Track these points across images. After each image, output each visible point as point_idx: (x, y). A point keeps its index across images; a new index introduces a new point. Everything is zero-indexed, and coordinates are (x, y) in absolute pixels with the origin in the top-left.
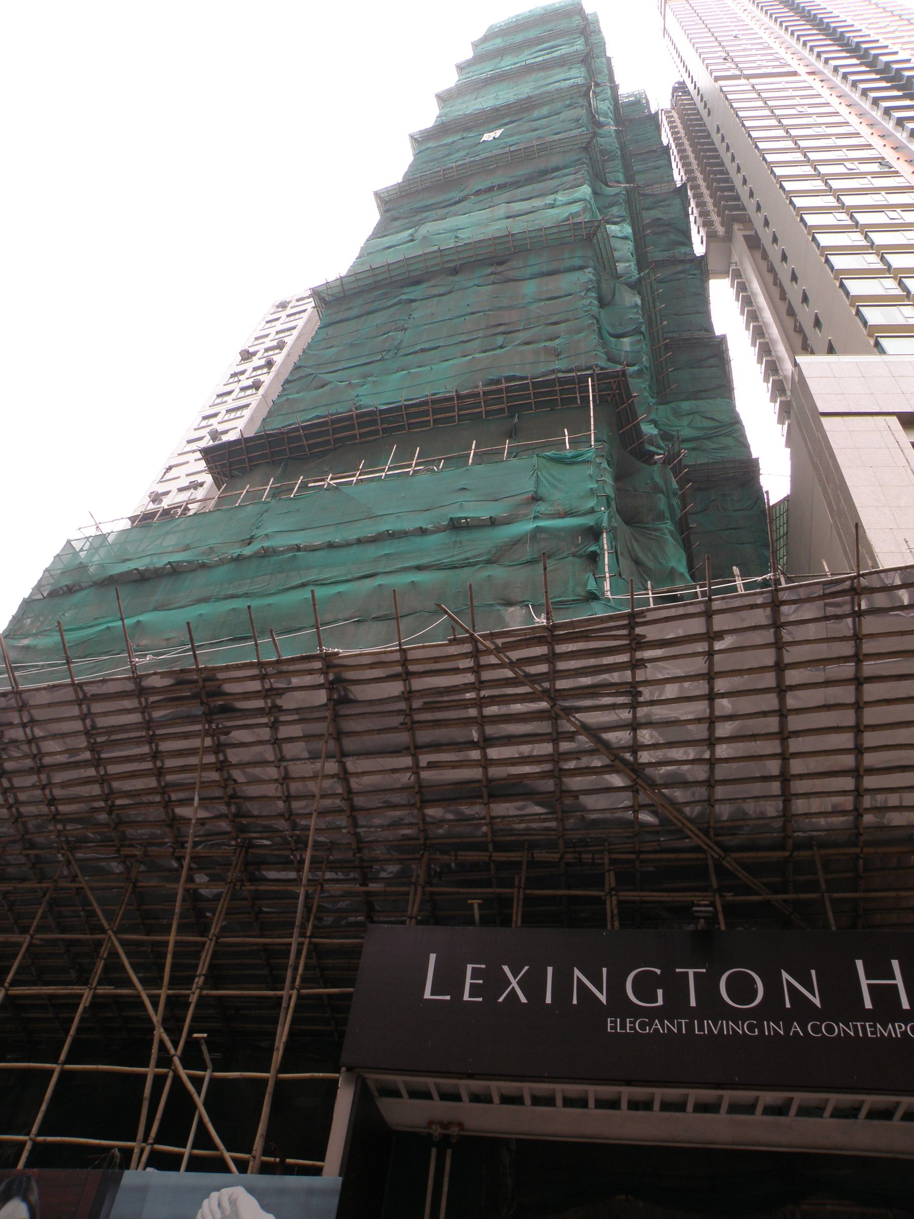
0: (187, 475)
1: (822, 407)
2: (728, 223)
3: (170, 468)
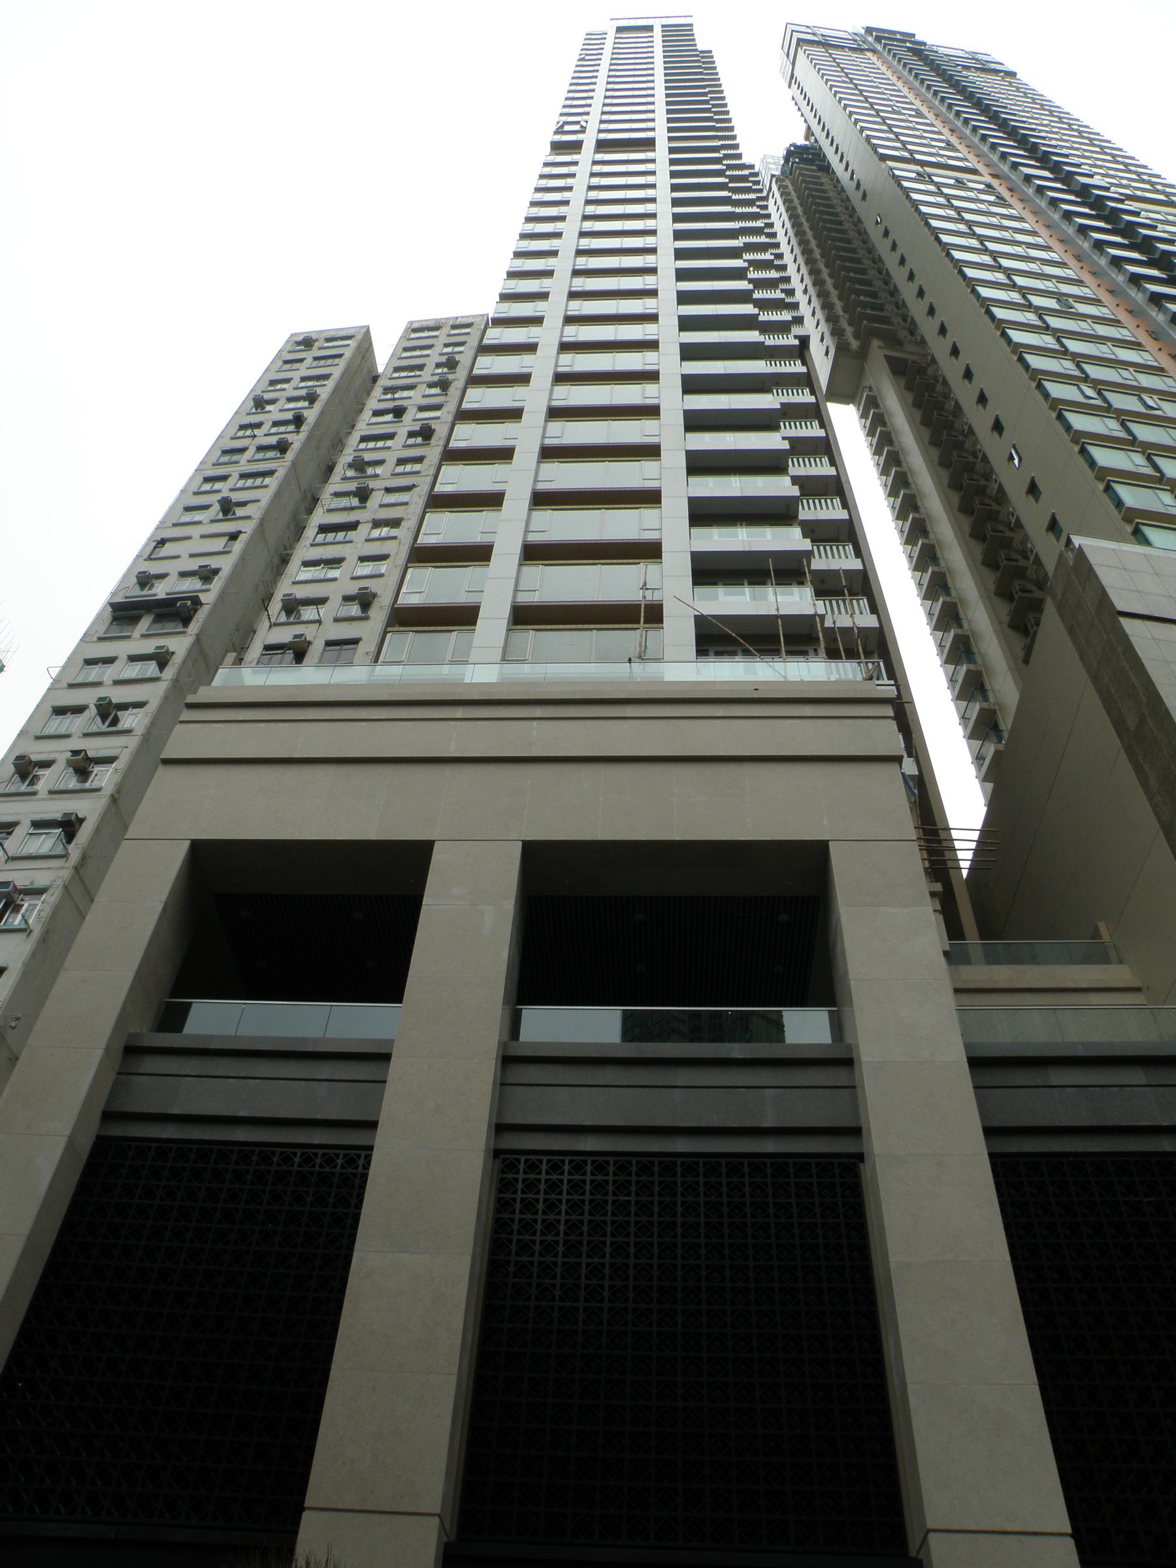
0: (191, 556)
1: (1120, 605)
2: (864, 338)
3: (162, 542)
